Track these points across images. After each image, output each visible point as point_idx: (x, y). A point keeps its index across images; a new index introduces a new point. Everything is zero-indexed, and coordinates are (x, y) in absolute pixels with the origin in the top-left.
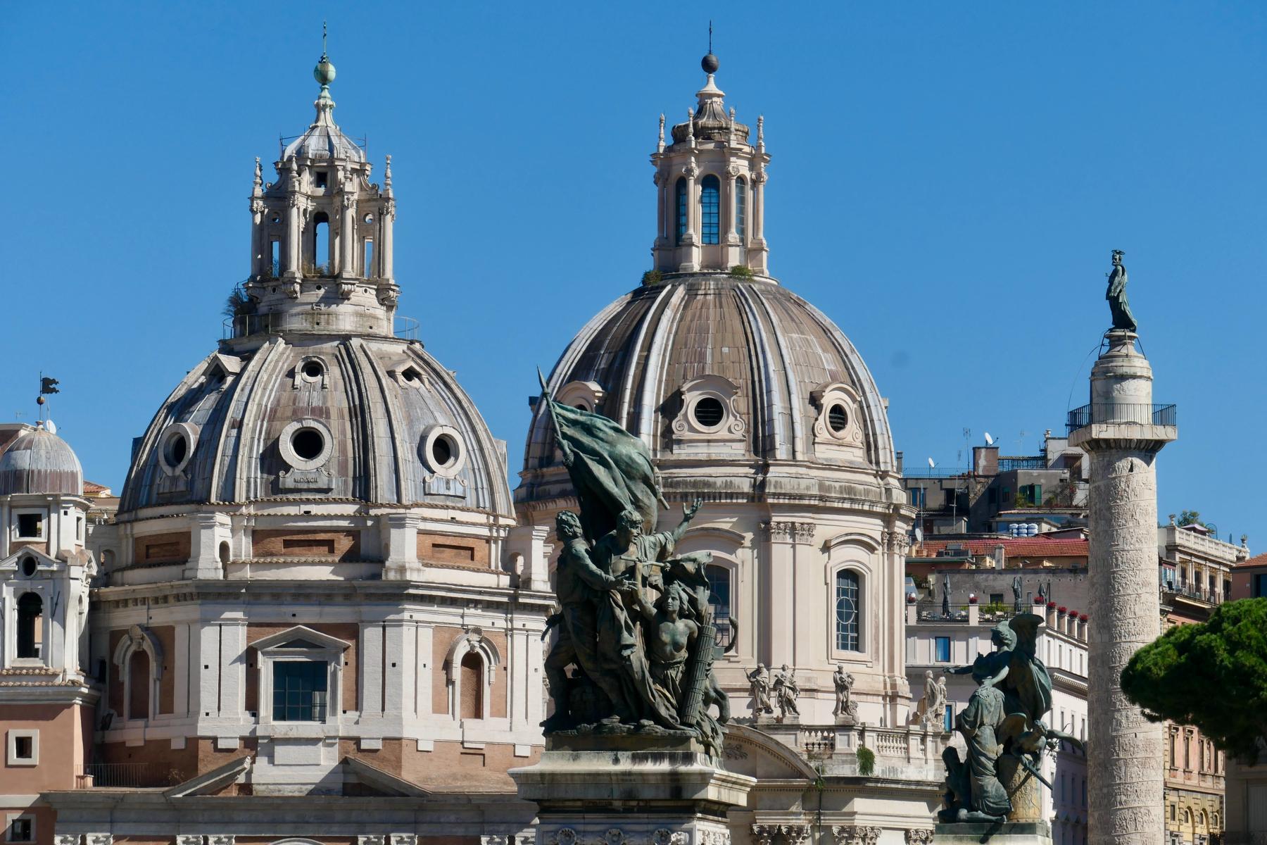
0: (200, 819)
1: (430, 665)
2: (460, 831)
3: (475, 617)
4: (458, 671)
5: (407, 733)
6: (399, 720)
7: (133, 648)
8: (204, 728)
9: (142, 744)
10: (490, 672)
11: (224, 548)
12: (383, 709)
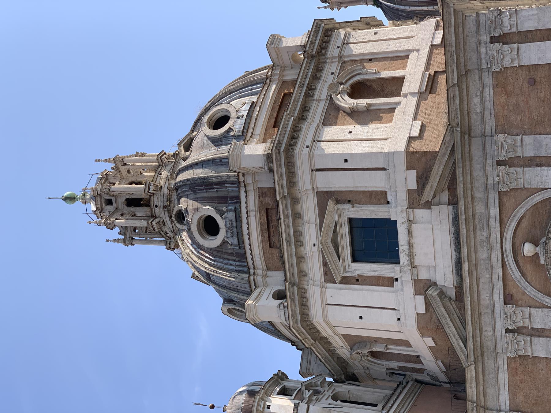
0: (490, 334)
1: (351, 128)
2: (489, 92)
3: (322, 91)
4: (362, 103)
5: (401, 147)
6: (391, 155)
7: (369, 358)
8: (411, 322)
9: (440, 363)
10: (371, 71)
11: (280, 295)
12: (383, 169)
